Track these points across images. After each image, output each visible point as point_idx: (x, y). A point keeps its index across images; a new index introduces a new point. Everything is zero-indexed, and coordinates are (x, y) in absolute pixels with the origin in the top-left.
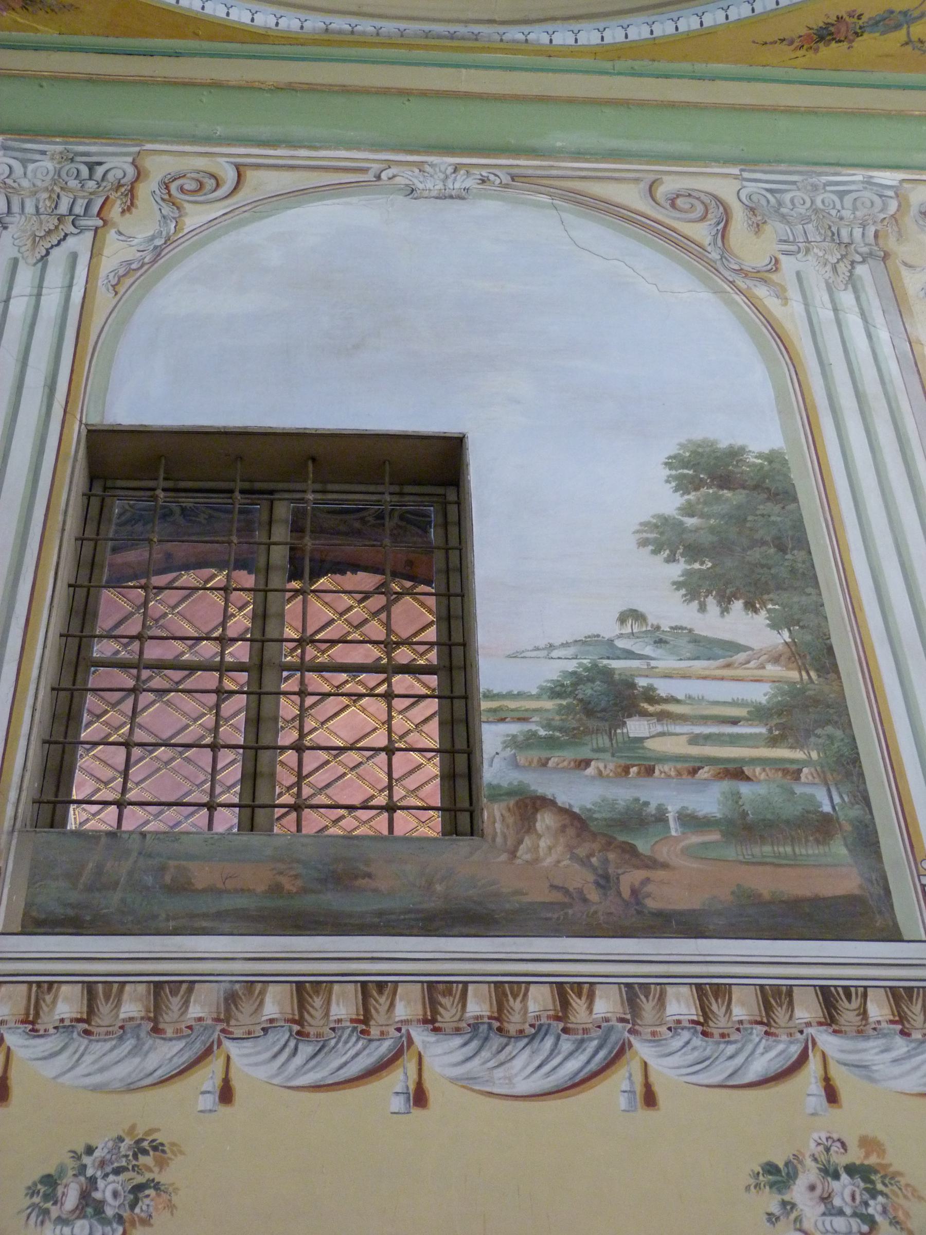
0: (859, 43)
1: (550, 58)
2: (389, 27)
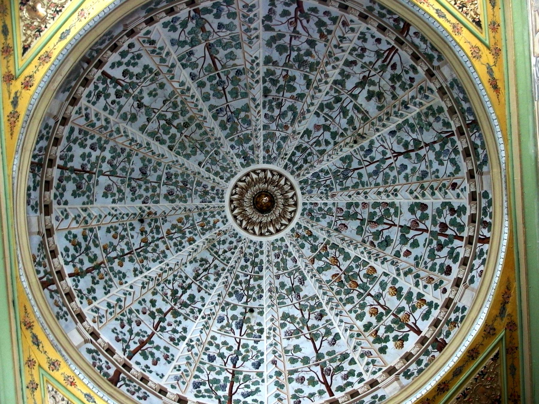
0: (496, 77)
1: (509, 156)
2: (505, 198)
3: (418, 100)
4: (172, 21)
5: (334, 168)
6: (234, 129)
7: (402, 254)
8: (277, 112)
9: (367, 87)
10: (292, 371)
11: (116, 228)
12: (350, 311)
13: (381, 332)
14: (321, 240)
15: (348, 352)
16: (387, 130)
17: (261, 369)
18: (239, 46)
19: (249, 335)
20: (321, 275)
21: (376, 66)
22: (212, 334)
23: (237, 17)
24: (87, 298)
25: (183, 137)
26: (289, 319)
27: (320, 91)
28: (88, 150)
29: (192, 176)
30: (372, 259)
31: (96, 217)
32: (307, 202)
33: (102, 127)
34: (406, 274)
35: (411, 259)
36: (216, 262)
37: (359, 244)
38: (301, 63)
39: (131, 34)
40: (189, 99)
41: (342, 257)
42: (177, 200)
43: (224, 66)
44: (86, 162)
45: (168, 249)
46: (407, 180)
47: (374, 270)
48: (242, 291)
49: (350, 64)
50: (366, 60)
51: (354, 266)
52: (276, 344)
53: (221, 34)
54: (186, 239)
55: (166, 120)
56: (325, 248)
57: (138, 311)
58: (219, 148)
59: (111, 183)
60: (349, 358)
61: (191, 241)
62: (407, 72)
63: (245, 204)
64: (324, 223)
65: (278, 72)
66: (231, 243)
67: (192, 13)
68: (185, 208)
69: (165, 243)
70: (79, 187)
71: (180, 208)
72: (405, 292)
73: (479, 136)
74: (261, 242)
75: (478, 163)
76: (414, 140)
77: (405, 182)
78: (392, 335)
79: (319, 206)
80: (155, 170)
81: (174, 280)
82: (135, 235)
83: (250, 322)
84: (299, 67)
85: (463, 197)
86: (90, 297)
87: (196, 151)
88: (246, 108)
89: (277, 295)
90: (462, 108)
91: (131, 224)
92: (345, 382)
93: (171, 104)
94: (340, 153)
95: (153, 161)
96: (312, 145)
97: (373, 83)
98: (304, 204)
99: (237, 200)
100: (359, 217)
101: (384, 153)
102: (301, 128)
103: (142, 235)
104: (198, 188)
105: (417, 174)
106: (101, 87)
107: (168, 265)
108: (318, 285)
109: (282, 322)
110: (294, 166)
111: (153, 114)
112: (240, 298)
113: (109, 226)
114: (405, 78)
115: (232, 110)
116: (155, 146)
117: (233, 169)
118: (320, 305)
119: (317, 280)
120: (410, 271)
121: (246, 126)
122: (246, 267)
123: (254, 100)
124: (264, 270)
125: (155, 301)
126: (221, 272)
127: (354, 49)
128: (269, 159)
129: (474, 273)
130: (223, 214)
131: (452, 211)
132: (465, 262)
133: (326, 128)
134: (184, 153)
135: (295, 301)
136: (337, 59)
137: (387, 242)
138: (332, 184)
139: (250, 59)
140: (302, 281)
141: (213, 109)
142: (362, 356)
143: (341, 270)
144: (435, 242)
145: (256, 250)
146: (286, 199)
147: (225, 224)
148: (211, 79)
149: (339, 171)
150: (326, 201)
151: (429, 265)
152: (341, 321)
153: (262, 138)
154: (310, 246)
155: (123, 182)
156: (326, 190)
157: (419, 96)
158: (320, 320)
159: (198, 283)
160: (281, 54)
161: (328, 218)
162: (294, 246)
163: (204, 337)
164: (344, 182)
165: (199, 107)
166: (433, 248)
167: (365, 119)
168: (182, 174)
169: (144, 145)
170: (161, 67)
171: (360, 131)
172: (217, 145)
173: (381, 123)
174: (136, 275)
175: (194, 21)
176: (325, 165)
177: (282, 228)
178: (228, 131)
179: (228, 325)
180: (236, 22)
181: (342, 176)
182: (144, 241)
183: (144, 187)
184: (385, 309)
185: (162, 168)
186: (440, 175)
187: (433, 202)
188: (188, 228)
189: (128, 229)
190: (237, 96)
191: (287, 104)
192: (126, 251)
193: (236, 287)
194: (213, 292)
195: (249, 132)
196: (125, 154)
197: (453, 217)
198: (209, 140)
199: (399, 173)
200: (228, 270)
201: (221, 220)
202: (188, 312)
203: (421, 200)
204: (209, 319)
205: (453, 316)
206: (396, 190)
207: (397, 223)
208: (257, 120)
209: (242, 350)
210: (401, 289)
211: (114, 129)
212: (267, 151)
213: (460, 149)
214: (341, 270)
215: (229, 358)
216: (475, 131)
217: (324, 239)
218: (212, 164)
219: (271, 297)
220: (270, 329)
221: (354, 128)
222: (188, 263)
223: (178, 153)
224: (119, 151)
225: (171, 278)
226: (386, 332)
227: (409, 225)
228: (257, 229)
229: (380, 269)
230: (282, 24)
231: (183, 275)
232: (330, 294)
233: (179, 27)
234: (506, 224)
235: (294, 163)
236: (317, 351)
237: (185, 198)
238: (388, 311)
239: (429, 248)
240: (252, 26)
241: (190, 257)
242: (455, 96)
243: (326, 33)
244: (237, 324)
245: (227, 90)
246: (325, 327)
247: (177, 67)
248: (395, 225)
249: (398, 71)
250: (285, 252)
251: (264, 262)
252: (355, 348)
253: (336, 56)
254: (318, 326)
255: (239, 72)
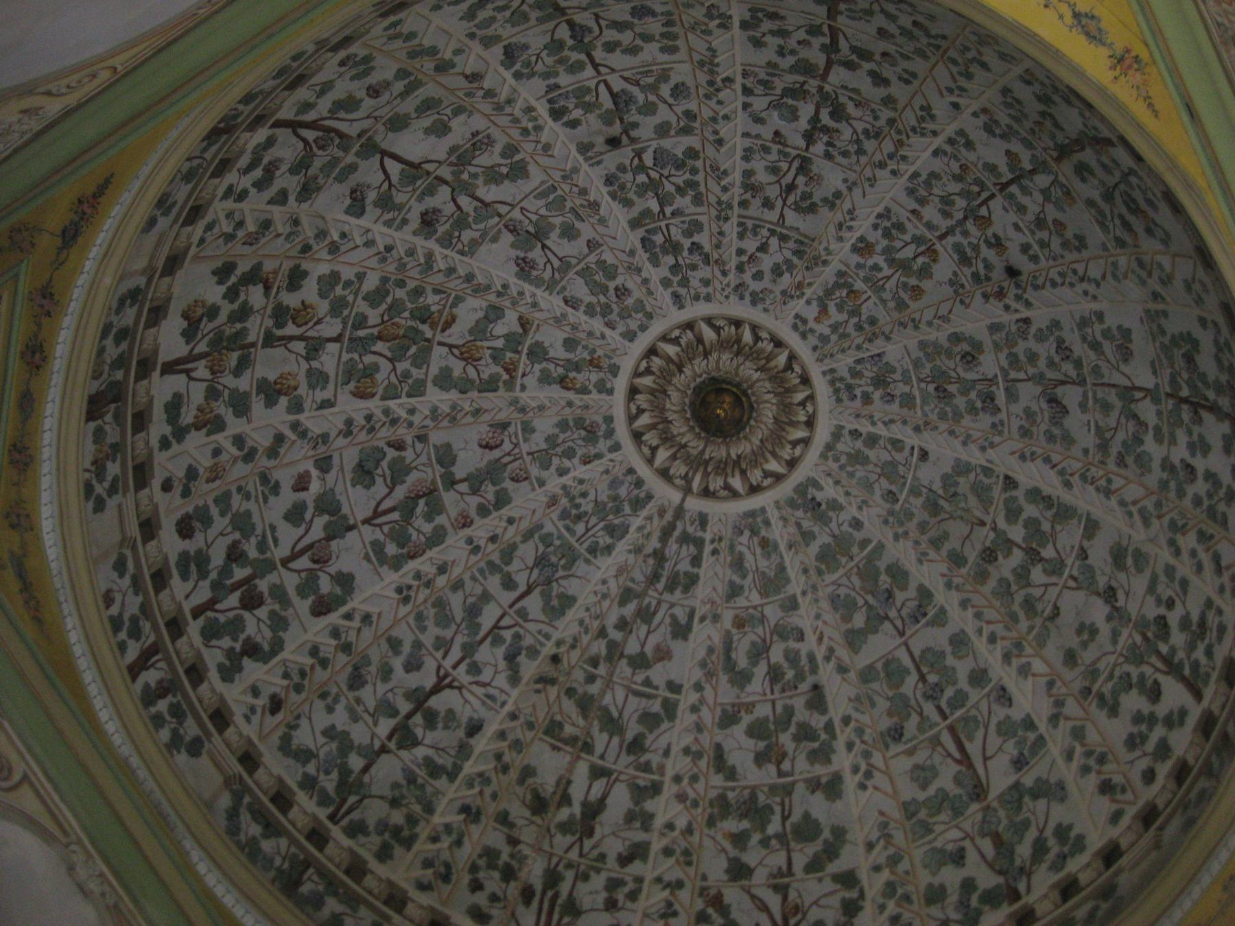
2: (150, 784)
3: (446, 842)
4: (1065, 857)
5: (581, 568)
6: (868, 573)
7: (315, 473)
8: (777, 654)
9: (577, 809)
10: (417, 88)
11: (1065, 244)
12: (361, 277)
13: (255, 296)
14: (531, 381)
15: (305, 206)
16: (490, 729)
17: (498, 50)
18: (909, 809)
19: (581, 92)
20: (485, 304)
21: (569, 875)
22: (682, 55)
23: (922, 887)
24: (1042, 84)
25: (988, 519)
26: (504, 170)
27: (686, 751)
28: (1199, 464)
29: (933, 417)
30: (378, 414)
31: (1125, 277)
32: (612, 456)
33: (1183, 530)
34: (279, 439)
35: (285, 477)
36: (773, 216)
37: (432, 424)
38: (753, 810)
39: (1149, 816)
40: (999, 629)
41: (457, 372)
42: (946, 344)
43: (936, 742)
44: (1196, 430)
45: (913, 212)
46: (389, 640)
47: (360, 395)
48: (666, 173)
49: (636, 853)
50: (598, 881)
51: (414, 371)
52: (499, 108)
53: (955, 834)
54: (879, 248)
55: (1042, 559)
56: (510, 369)
57: (906, 57)
58: (891, 513)
59: (1122, 367)
60: (292, 198)
61: (863, 247)
62: (494, 898)
63: (768, 385)
64: (544, 426)
65: (802, 764)
66: (758, 276)
67: (1022, 887)
68: (916, 327)
69: (929, 226)
70: (1189, 359)
71: (930, 324)
72: (257, 405)
73: (271, 861)
74: (681, 307)
75: (247, 799)
76: (416, 743)
77: (395, 633)
78: (226, 309)
79: (576, 461)
80: (1029, 414)
81: (858, 141)
82: (1012, 233)
83: (600, 116)
84: (753, 796)
85: (243, 698)
86: (1037, 85)
87: (944, 487)
88: (854, 639)
89: (569, 204)
90: (336, 894)
91: (1035, 259)
92: (265, 161)
93: (1039, 607)
94: (582, 614)
95: (1042, 438)
96: (659, 603)
97: (565, 828)
98: (616, 447)
99: (790, 391)
100: (463, 487)
101: (475, 669)
102: (705, 635)
103: (995, 235)
104: (907, 389)
105: (373, 669)
106: (1199, 654)
107: (894, 173)
108: (480, 279)
109: (517, 158)
110: (684, 532)
111: (1075, 573)
112: (661, 157)
113: (1085, 254)
114: (492, 882)
115: (887, 626)
116: (1051, 484)
117: (835, 466)
118: (446, 242)
119: (488, 287)
120: (273, 453)
121: (842, 591)
122: (688, 233)
123: (842, 669)
124: (638, 245)
125: (875, 84)
126: (748, 196)
127: (633, 896)
128: (753, 523)
129: (127, 581)
130: (812, 340)
131: (252, 650)
132: (160, 579)
133: (640, 662)
134: (972, 476)
135: (516, 214)
136: (668, 852)
137: (364, 474)
138: (568, 529)
139: (879, 779)
140: (524, 268)
141: (936, 615)
142: (266, 225)
143: (440, 344)
144: (253, 553)
145: (685, 283)
146: (667, 438)
147: (797, 316)
148: (960, 699)
149: (564, 568)
150: (565, 480)
151: (236, 500)
152: (369, 244)
153: (791, 573)
154: (552, 354)
155: (1096, 370)
156: (578, 506)
157: (446, 856)
158: (424, 215)
159: (794, 152)
160: (806, 815)
161: (538, 441)
162: (590, 334)
163: (698, 43)
164: (541, 548)
165: (970, 611)
166: (246, 536)
167: (553, 729)
168: (957, 416)
169: (1075, 480)
170: (1081, 714)
171: (553, 692)
172: (896, 518)
173: (511, 737)
174: (961, 133)
175: (1018, 862)
176: (606, 566)
177: (644, 364)
178: (882, 565)
179: (654, 88)
180: (924, 878)
181: (554, 559)
182: (985, 222)
183: (1042, 363)
184: (282, 338)
185: (1015, 423)
186: (320, 705)
187: (307, 631)
188: (888, 278)
189: (1036, 247)
190: (887, 665)
191: (758, 684)
192: (1014, 189)
193: (687, 176)
194: (740, 144)
195: (829, 578)
196: (1115, 449)
197: (242, 637)
198: (923, 527)
199: (418, 645)
200: (730, 207)
201: (811, 324)
202: (776, 79)
203: (334, 618)
204: (711, 83)
205: (113, 469)
206: (406, 600)
207: (366, 530)
208: (818, 617)
209: (575, 56)
210: (270, 402)
211: (1155, 522)
212: (764, 543)
213: (302, 797)
214: (440, 344)
215: (596, 29)
216: (286, 866)
217: (523, 388)
218: (893, 464)
219: (584, 192)
220: (538, 128)
221: (570, 692)
222: (845, 192)
223: (987, 471)
224: (1130, 460)
225: (870, 145)
226: (245, 302)
227: (334, 544)
228: (708, 334)
229: (350, 406)
230: (816, 903)
231: (840, 159)
232: (438, 279)
233: (1051, 842)
234: (117, 739)
235: (685, 539)
236: (385, 153)
237: (927, 355)
238: (270, 340)
239: (259, 531)
240: (885, 875)
241: (847, 205)
242: (363, 911)
243: (710, 911)
244: (630, 99)
245: (913, 678)
246: (400, 208)
247: (1045, 719)
248: (367, 521)
249: (513, 889)
250: (606, 310)
251: (647, 264)
252: (296, 222)
253: (672, 861)
254: (420, 199)
255: (897, 734)
